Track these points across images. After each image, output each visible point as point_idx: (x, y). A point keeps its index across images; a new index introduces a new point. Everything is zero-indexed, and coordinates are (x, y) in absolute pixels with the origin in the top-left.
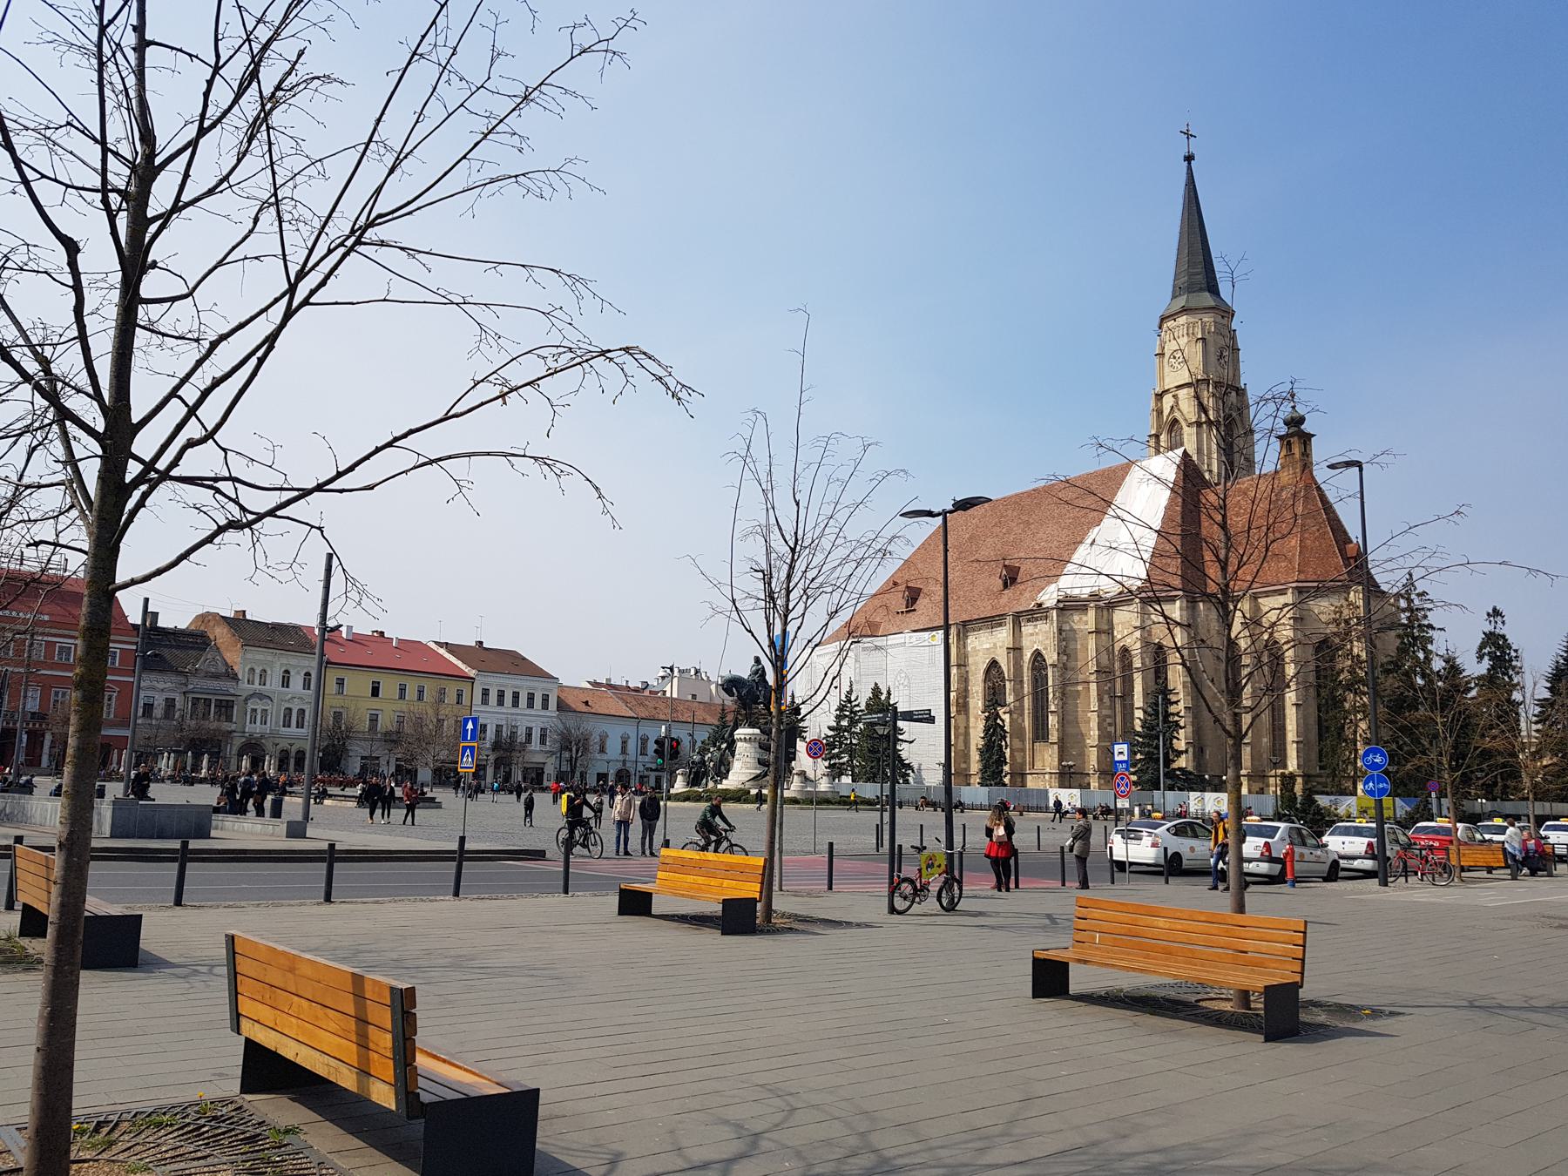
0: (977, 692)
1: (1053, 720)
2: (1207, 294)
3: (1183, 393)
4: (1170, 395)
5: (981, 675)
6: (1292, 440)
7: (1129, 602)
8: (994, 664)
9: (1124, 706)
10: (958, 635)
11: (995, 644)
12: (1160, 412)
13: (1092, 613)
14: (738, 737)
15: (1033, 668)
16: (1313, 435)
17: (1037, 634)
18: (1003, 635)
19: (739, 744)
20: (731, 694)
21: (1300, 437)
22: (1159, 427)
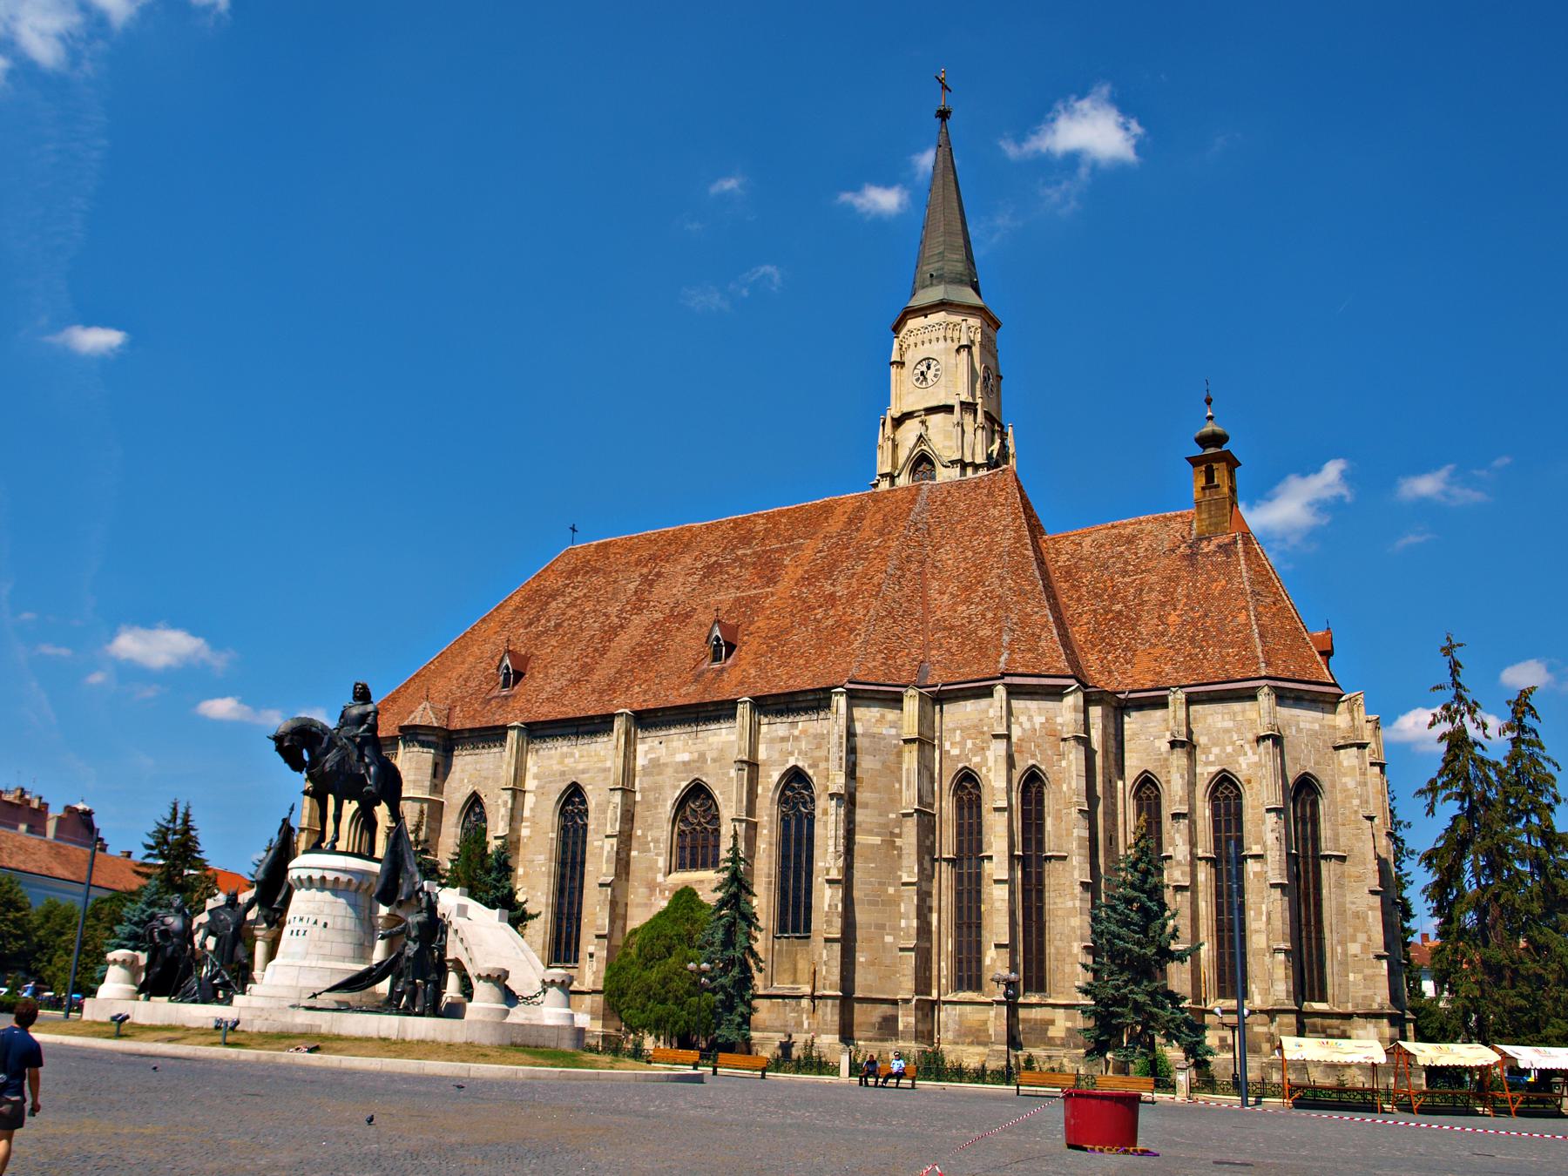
0: (656, 841)
1: (826, 899)
2: (971, 289)
3: (936, 420)
4: (919, 419)
5: (667, 809)
6: (1215, 466)
7: (987, 692)
8: (698, 792)
9: (959, 879)
10: (627, 733)
11: (702, 756)
12: (895, 446)
13: (911, 705)
14: (304, 874)
15: (783, 800)
16: (1240, 464)
17: (796, 738)
18: (725, 737)
19: (299, 896)
20: (296, 764)
21: (1228, 463)
22: (894, 465)
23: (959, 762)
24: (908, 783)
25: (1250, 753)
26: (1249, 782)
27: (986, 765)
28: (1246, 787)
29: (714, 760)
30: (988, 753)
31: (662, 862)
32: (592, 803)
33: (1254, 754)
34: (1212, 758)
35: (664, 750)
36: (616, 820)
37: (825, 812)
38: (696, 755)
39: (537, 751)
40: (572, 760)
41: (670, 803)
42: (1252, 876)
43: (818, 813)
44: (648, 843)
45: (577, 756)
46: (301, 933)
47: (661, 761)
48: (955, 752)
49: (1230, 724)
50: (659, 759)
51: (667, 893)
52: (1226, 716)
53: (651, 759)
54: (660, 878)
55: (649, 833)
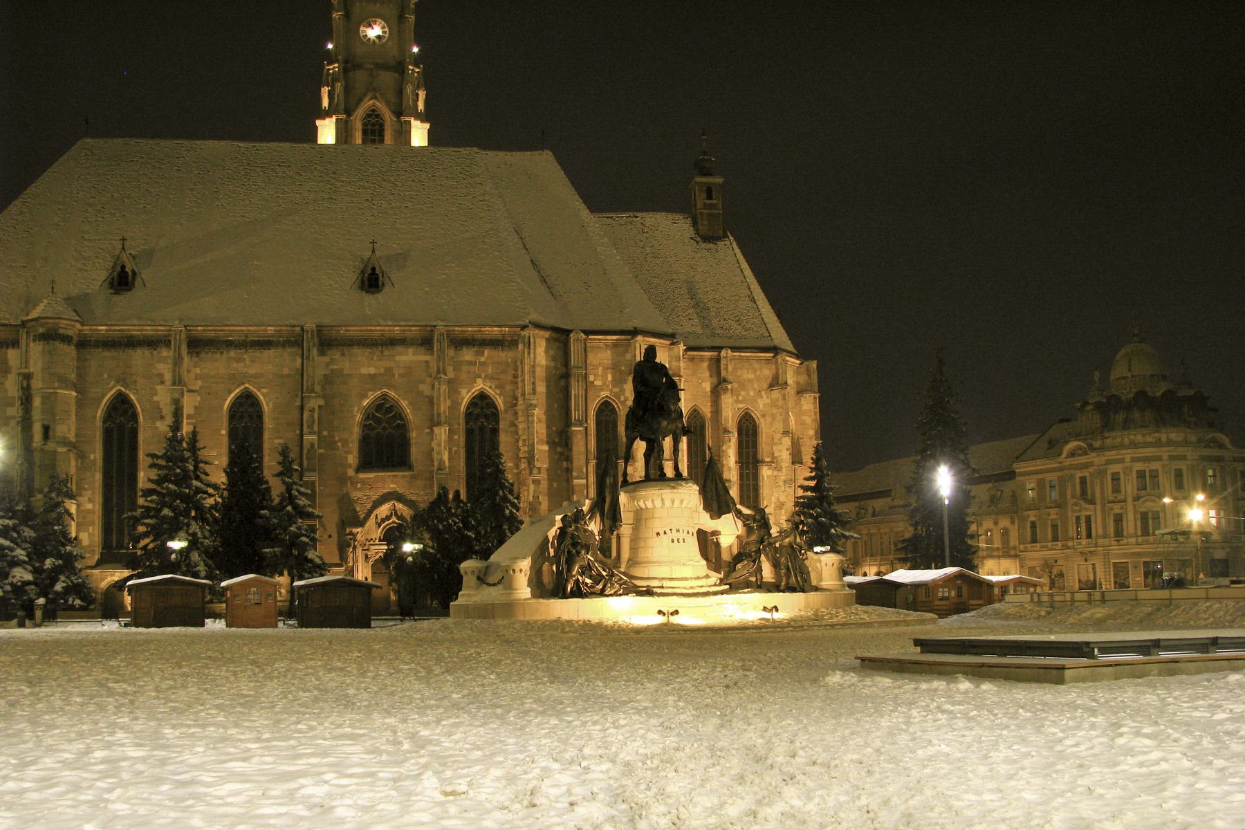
0: (345, 442)
15: (468, 415)
17: (483, 364)
23: (602, 390)
24: (577, 405)
25: (765, 397)
26: (764, 416)
27: (624, 394)
28: (762, 420)
29: (402, 376)
30: (625, 386)
31: (353, 459)
32: (266, 407)
33: (767, 398)
34: (740, 398)
35: (347, 363)
36: (313, 422)
37: (513, 425)
38: (382, 371)
39: (198, 354)
40: (243, 364)
41: (356, 409)
42: (766, 478)
43: (502, 425)
44: (336, 442)
45: (248, 362)
46: (681, 540)
47: (345, 372)
48: (598, 383)
49: (752, 376)
50: (342, 370)
51: (359, 485)
52: (750, 371)
53: (332, 370)
54: (351, 472)
55: (336, 434)
